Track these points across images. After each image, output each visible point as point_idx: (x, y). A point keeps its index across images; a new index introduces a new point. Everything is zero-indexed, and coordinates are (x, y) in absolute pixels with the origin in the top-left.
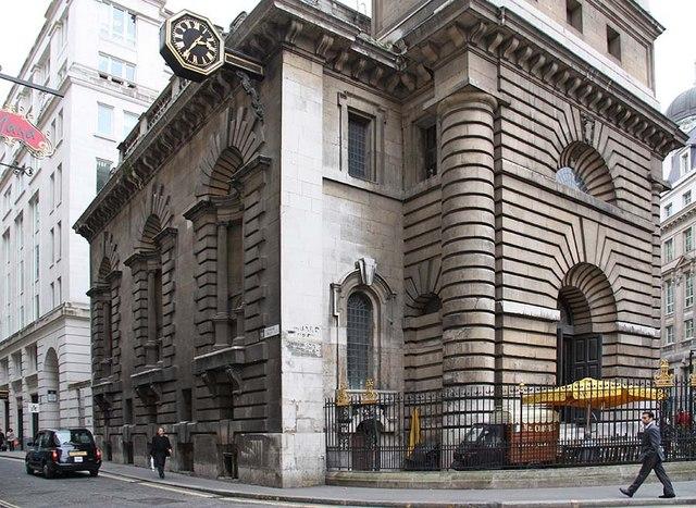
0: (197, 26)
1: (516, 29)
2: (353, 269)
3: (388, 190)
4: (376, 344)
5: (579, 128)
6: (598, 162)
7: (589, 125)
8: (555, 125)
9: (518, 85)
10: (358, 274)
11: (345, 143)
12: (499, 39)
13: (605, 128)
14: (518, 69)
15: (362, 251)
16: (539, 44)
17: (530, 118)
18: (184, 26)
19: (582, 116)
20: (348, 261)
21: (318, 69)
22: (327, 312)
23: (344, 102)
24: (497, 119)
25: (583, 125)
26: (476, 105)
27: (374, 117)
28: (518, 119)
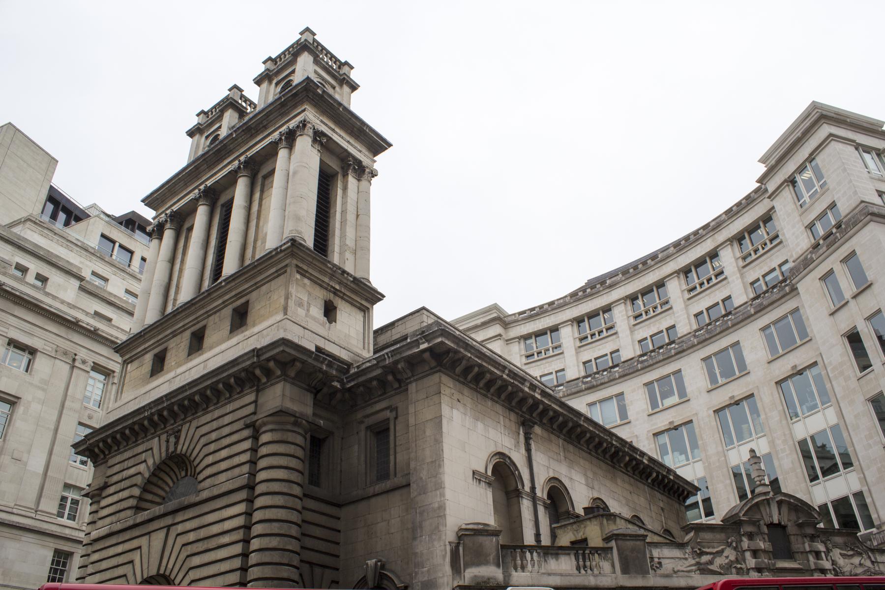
13: (195, 424)
28: (112, 490)
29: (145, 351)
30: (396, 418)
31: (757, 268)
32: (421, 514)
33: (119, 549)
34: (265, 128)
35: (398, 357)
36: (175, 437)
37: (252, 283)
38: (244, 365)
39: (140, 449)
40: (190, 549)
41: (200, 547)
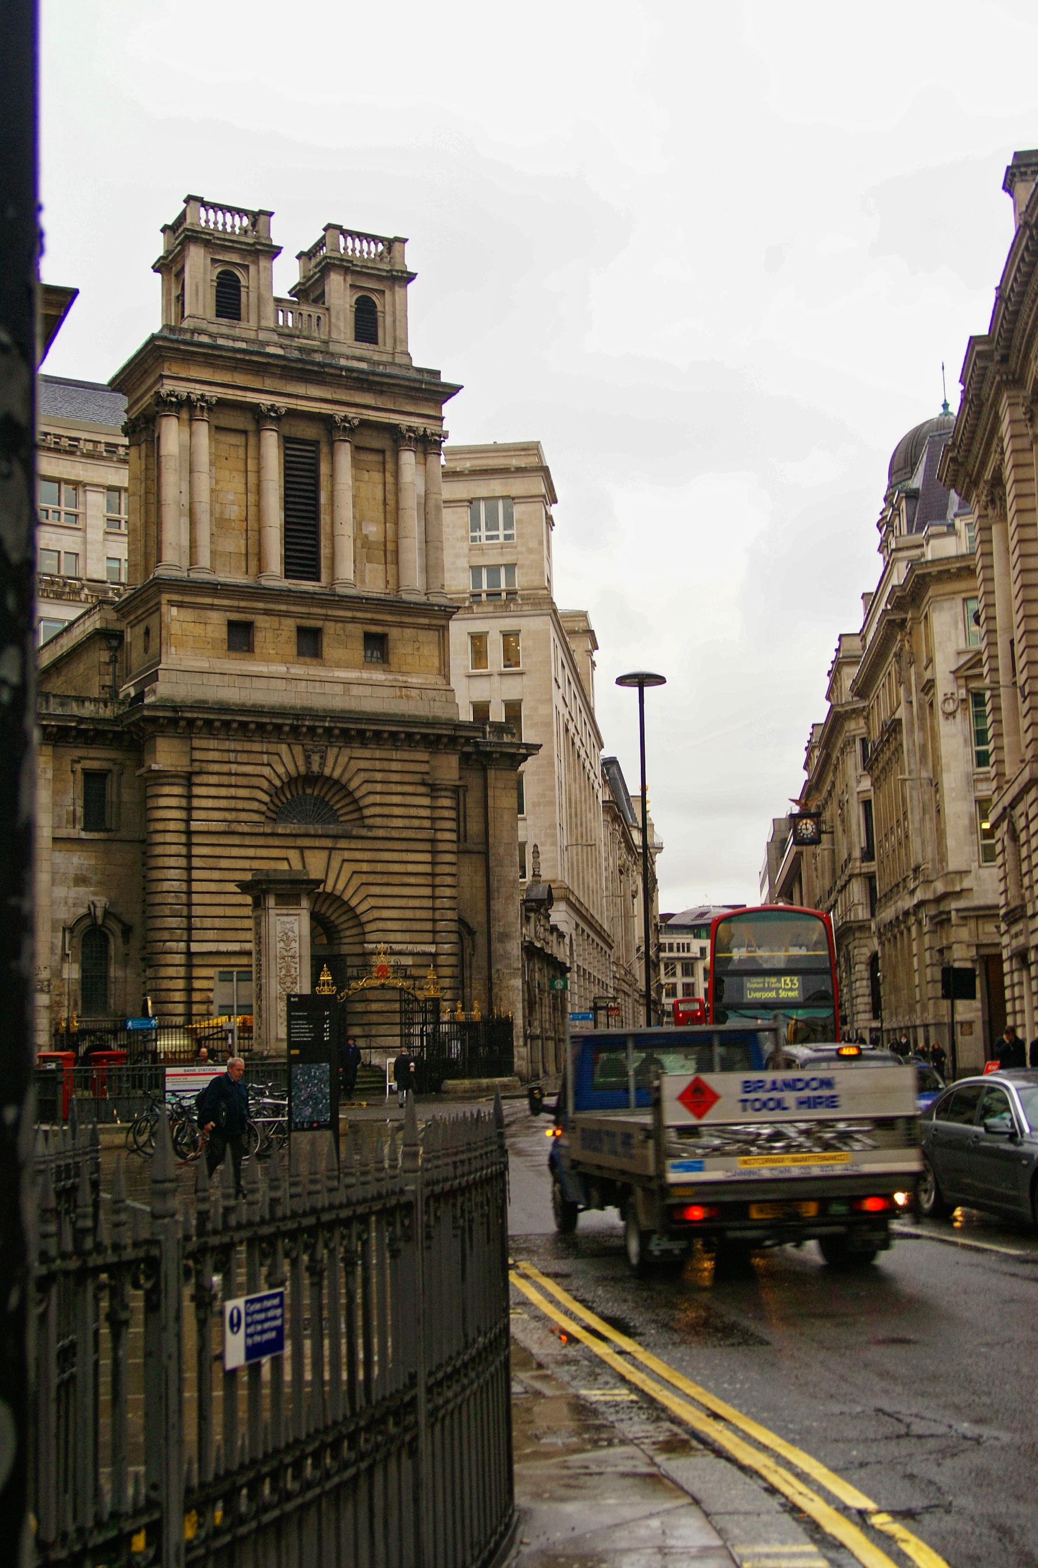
1: (195, 715)
3: (123, 834)
4: (112, 974)
5: (301, 762)
6: (339, 786)
7: (316, 758)
8: (266, 771)
9: (211, 750)
12: (183, 723)
13: (347, 752)
14: (215, 737)
15: (95, 894)
16: (223, 717)
17: (230, 774)
19: (305, 750)
20: (82, 906)
22: (59, 951)
23: (78, 767)
24: (190, 785)
25: (308, 759)
26: (165, 780)
27: (110, 771)
28: (213, 779)
29: (212, 607)
32: (499, 881)
33: (251, 852)
34: (382, 393)
36: (321, 757)
38: (440, 732)
39: (257, 747)
40: (365, 878)
41: (378, 879)
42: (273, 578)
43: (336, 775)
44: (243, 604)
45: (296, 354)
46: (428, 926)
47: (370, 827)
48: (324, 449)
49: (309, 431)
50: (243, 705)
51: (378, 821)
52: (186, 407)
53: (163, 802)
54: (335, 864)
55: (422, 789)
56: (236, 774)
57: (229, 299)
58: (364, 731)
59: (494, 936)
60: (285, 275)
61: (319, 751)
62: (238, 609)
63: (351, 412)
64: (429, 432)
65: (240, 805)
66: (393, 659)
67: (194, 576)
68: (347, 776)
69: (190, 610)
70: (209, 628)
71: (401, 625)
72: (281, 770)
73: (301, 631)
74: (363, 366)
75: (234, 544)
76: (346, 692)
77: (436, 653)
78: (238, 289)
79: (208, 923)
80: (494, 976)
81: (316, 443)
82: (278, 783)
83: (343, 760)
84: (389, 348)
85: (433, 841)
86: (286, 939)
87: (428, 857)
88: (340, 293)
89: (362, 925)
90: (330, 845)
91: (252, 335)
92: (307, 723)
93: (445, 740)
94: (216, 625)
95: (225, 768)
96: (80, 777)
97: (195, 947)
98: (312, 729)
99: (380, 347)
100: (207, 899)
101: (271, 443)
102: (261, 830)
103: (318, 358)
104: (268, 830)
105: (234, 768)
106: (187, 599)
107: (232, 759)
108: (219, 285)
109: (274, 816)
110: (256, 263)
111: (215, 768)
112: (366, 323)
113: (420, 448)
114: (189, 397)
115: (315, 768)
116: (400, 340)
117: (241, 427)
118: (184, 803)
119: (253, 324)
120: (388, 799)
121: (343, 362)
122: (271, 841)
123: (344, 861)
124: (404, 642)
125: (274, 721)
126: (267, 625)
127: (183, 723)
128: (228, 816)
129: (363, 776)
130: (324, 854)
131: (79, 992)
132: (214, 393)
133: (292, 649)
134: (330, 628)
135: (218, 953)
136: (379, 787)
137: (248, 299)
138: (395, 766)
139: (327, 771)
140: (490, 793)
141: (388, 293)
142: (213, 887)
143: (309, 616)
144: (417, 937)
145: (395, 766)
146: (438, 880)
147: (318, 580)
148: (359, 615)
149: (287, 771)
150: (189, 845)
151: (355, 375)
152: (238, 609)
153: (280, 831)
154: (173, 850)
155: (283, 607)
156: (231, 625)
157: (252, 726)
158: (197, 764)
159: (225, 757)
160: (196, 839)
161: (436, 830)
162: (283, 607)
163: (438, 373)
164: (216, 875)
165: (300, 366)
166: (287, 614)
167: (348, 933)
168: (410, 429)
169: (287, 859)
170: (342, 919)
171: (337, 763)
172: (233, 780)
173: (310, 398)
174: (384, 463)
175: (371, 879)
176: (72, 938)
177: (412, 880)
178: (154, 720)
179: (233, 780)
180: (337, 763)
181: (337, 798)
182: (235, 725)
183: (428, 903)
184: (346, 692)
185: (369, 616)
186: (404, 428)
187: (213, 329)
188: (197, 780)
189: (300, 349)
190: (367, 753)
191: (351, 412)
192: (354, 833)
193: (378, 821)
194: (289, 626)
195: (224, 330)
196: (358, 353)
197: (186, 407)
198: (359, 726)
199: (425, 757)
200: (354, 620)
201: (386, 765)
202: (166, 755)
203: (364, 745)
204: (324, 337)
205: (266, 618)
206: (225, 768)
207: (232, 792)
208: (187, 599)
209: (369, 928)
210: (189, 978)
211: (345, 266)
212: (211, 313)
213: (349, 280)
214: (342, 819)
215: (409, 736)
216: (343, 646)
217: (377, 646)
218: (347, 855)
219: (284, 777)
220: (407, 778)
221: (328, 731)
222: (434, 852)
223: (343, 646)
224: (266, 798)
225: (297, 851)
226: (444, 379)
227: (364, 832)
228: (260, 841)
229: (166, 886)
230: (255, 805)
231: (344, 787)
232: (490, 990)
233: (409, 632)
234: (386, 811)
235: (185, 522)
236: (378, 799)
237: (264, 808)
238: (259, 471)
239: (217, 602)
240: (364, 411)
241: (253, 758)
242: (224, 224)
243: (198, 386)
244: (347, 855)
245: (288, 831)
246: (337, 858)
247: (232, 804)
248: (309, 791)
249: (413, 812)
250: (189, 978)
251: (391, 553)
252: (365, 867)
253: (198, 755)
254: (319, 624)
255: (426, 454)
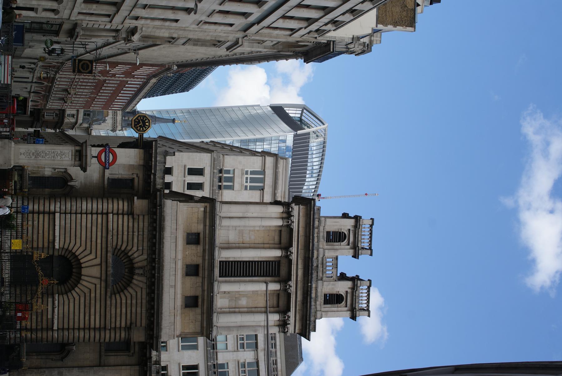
0: (147, 124)
1: (158, 215)
2: (74, 178)
5: (139, 264)
6: (129, 283)
7: (141, 271)
8: (135, 249)
9: (144, 224)
10: (72, 179)
11: (120, 177)
12: (154, 210)
13: (144, 286)
14: (149, 225)
15: (81, 183)
16: (158, 227)
17: (133, 232)
18: (146, 120)
19: (144, 267)
21: (142, 162)
23: (135, 176)
25: (141, 268)
26: (130, 203)
28: (131, 224)
29: (205, 226)
30: (128, 356)
31: (234, 369)
33: (99, 241)
35: (148, 369)
36: (142, 274)
37: (205, 311)
38: (155, 329)
39: (145, 244)
40: (88, 295)
41: (88, 302)
42: (219, 254)
43: (134, 281)
44: (207, 239)
45: (315, 264)
46: (66, 326)
47: (111, 298)
48: (276, 279)
49: (283, 271)
50: (163, 238)
51: (114, 301)
52: (288, 215)
53: (121, 203)
54: (94, 281)
55: (129, 322)
56: (133, 235)
57: (336, 237)
58: (154, 293)
59: (61, 370)
60: (348, 264)
61: (144, 273)
62: (205, 237)
63: (293, 289)
64: (288, 326)
65: (120, 237)
66: (187, 309)
67: (217, 218)
68: (133, 286)
69: (203, 216)
70: (196, 225)
71: (202, 313)
72: (135, 255)
73: (197, 266)
74: (313, 295)
75: (233, 237)
76: (171, 286)
77: (191, 331)
78: (339, 241)
79: (68, 221)
80: (42, 370)
81: (279, 275)
82: (130, 254)
83: (141, 285)
84: (323, 309)
85: (105, 328)
86: (62, 154)
87: (97, 325)
88: (343, 287)
89: (66, 293)
90: (103, 278)
91: (321, 246)
92: (157, 265)
93: (151, 333)
94: (198, 228)
95: (136, 230)
96: (132, 177)
97: (57, 215)
98: (154, 268)
99: (323, 306)
100: (79, 221)
101: (277, 253)
102: (109, 246)
103: (314, 275)
104: (109, 249)
105: (136, 234)
106: (208, 214)
107: (140, 233)
108: (340, 233)
109: (115, 254)
110: (351, 248)
111: (136, 225)
112: (334, 299)
113: (281, 323)
114: (292, 216)
115: (137, 271)
116: (326, 314)
117: (282, 241)
118: (120, 212)
119: (326, 247)
120: (124, 306)
121: (314, 286)
122: (104, 250)
123: (96, 285)
124: (195, 314)
125: (157, 250)
126: (198, 251)
127: (154, 210)
128: (115, 231)
129: (134, 294)
130: (98, 275)
131: (39, 175)
132: (295, 226)
133: (189, 262)
134: (199, 280)
135: (54, 225)
136: (129, 302)
137: (337, 245)
138: (139, 309)
139: (135, 277)
140: (128, 367)
141: (346, 309)
142: (84, 224)
143: (204, 269)
144: (61, 320)
145: (139, 309)
146: (87, 331)
147: (220, 277)
148: (206, 293)
149: (135, 258)
150: (102, 213)
151: (309, 289)
152: (205, 237)
153: (108, 254)
154: (100, 206)
155: (207, 258)
156: (198, 234)
157: (154, 241)
158: (137, 217)
159: (141, 230)
160: (104, 216)
161: (110, 330)
162: (207, 258)
163: (315, 331)
164: (89, 225)
165: (310, 265)
166: (204, 259)
167: (63, 289)
168: (289, 317)
169: (96, 258)
170: (69, 285)
171: (140, 281)
172: (131, 233)
173: (297, 271)
174: (273, 307)
175: (88, 298)
176: (62, 172)
177: (87, 318)
178: (156, 198)
179: (131, 233)
180: (140, 281)
181: (124, 283)
182: (154, 233)
183: (76, 326)
184: (171, 286)
185: (206, 298)
186: (289, 314)
187: (321, 228)
188: (130, 217)
189: (317, 266)
190: (144, 296)
191: (293, 289)
192: (108, 290)
193: (114, 301)
194: (199, 261)
195: (321, 234)
196: (319, 294)
197: (288, 215)
198: (156, 290)
199: (144, 325)
200: (203, 291)
201: (139, 305)
202: (139, 204)
203: (148, 294)
204: (324, 279)
205: (202, 250)
206: (136, 230)
207: (126, 233)
208: (208, 214)
209: (65, 297)
210: (44, 213)
211: (354, 288)
212: (328, 229)
213: (349, 291)
214: (114, 286)
215: (153, 315)
216: (192, 286)
217: (191, 302)
218: (98, 286)
219: (133, 256)
220: (134, 316)
221: (154, 276)
222: (100, 329)
223: (192, 286)
224: (123, 248)
225: (99, 263)
226: (312, 334)
227: (109, 294)
228: (104, 245)
229: (84, 204)
230: (120, 243)
231: (129, 285)
232: (36, 368)
233: (199, 317)
234: (119, 305)
235: (241, 215)
236: (124, 301)
237: (119, 247)
238: (264, 248)
239: (207, 227)
240: (294, 295)
241: (140, 243)
242: (364, 235)
243: (297, 220)
244: (98, 286)
245: (108, 258)
246: (97, 281)
247: (120, 233)
248: (127, 270)
249: (118, 319)
250: (44, 213)
251: (234, 311)
252: (93, 295)
253: (141, 217)
254: (201, 274)
255: (279, 326)
